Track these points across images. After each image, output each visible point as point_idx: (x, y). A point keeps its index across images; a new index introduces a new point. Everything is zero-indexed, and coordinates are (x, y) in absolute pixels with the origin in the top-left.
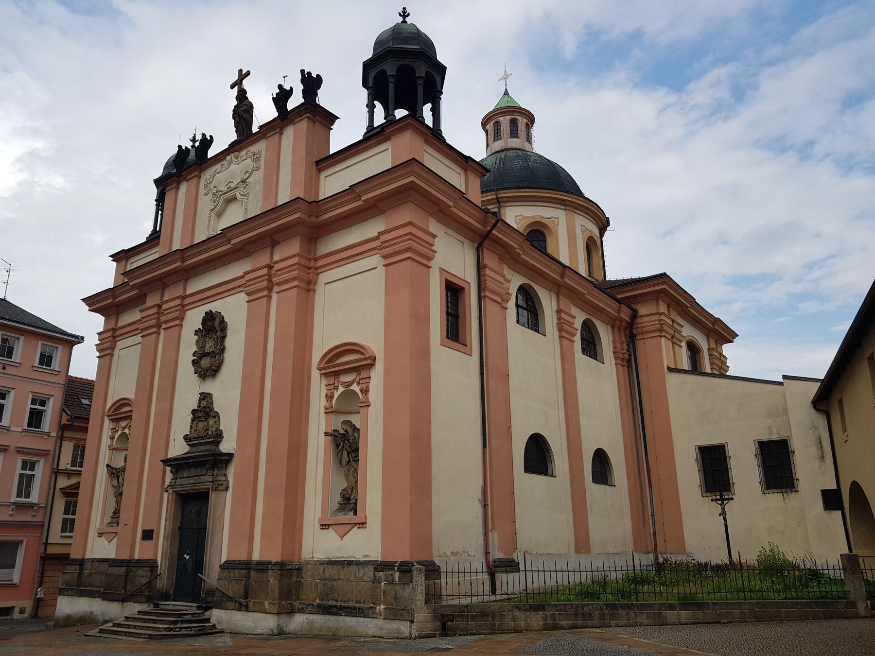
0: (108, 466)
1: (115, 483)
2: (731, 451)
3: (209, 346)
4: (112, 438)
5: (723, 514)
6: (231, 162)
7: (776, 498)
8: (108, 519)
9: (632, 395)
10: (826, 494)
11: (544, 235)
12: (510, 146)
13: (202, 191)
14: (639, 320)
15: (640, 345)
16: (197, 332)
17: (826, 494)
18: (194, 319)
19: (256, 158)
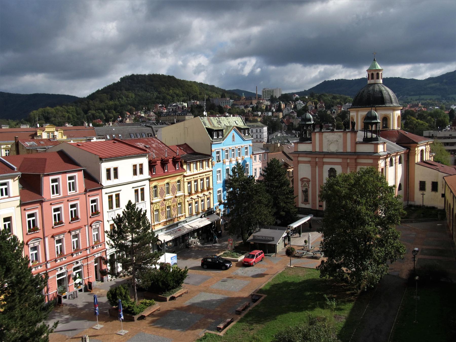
0: (302, 190)
1: (305, 194)
2: (426, 183)
3: (332, 174)
4: (302, 185)
5: (423, 197)
6: (332, 135)
7: (433, 193)
8: (303, 200)
9: (407, 168)
10: (442, 194)
11: (387, 118)
12: (376, 83)
13: (324, 138)
14: (410, 151)
15: (410, 157)
16: (329, 171)
17: (442, 194)
18: (326, 168)
19: (340, 136)
